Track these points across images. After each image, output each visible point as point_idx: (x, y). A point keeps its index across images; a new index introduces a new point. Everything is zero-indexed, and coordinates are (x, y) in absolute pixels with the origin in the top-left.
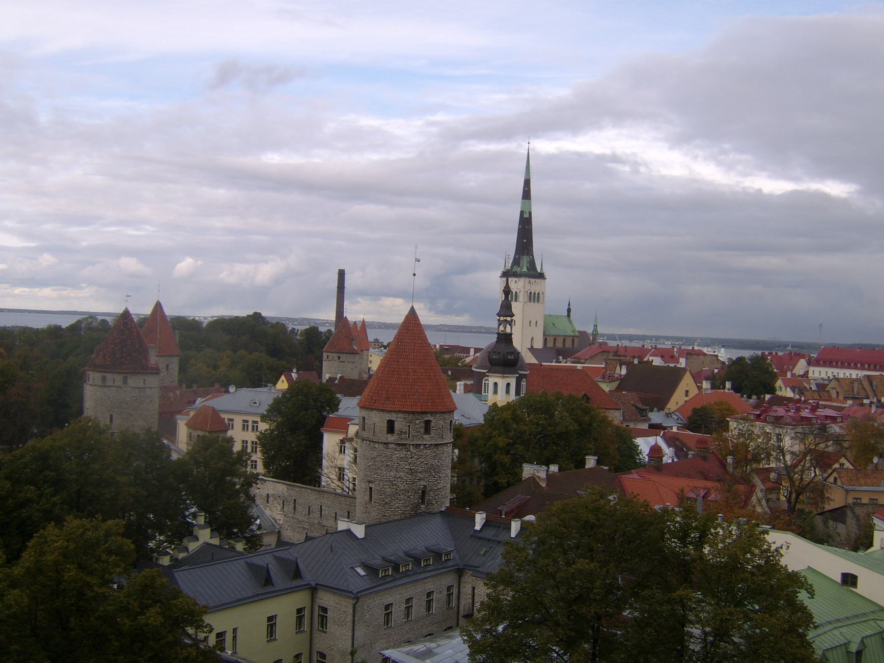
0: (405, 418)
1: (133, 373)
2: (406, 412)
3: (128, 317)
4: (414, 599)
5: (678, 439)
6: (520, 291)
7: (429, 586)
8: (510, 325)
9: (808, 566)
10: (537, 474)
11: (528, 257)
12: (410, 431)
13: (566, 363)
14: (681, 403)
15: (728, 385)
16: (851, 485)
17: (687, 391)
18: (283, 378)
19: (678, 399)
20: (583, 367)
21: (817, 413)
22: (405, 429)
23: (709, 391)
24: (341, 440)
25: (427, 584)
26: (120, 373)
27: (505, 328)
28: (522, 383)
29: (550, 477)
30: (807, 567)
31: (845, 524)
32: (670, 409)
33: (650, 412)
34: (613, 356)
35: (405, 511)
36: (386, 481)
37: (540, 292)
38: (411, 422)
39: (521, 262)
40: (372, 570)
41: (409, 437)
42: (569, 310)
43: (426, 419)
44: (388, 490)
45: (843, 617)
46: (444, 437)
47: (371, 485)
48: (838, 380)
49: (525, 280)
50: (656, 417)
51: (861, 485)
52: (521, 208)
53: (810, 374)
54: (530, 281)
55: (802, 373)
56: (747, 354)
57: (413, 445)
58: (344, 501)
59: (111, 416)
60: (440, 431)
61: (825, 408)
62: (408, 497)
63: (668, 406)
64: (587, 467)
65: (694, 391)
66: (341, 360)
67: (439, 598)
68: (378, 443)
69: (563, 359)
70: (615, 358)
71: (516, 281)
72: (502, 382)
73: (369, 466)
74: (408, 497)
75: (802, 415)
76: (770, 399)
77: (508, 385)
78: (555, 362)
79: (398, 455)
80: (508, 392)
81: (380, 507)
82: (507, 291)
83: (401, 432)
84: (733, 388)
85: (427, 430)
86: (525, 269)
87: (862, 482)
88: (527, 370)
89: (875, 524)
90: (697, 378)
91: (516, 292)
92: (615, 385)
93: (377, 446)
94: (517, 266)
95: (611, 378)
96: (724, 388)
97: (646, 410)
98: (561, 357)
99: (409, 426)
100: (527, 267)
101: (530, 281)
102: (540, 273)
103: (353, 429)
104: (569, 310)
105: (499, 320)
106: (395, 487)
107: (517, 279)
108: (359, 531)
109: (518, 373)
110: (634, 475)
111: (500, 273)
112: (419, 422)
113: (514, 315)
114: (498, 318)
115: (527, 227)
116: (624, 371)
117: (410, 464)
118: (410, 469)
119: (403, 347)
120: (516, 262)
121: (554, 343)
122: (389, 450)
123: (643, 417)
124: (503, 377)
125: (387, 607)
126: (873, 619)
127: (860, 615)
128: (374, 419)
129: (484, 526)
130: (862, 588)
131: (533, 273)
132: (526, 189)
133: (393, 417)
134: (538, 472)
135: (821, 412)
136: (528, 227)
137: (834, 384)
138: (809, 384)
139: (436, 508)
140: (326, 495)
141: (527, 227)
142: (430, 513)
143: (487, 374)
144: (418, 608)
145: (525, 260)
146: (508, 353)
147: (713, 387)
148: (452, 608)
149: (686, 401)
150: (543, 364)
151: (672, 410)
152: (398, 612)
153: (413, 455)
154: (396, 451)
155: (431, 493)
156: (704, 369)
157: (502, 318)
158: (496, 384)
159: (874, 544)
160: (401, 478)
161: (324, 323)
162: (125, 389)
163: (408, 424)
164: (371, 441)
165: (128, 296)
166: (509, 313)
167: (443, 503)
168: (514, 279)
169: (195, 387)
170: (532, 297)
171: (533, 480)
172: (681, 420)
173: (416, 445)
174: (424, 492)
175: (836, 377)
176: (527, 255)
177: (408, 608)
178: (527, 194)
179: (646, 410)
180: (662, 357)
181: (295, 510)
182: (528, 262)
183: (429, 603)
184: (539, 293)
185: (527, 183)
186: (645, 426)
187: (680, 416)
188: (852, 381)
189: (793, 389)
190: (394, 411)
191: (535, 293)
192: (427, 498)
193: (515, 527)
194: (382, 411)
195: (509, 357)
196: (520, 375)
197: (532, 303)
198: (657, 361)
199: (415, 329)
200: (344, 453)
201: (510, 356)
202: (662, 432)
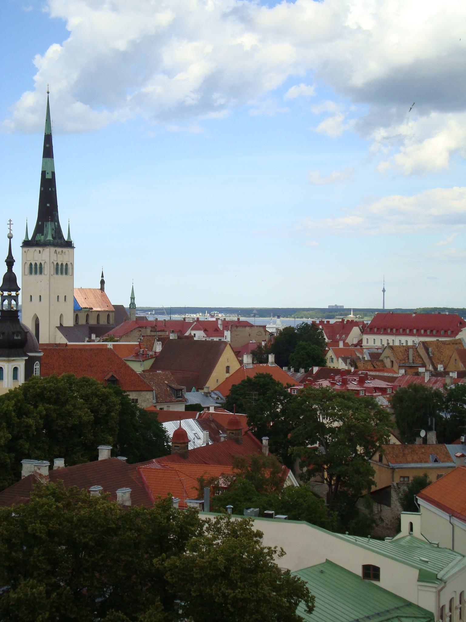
5: (213, 421)
6: (45, 262)
8: (15, 300)
9: (327, 560)
10: (38, 471)
11: (53, 224)
13: (99, 341)
16: (396, 462)
17: (228, 368)
21: (365, 385)
23: (251, 366)
27: (10, 304)
28: (35, 367)
29: (53, 474)
30: (325, 561)
31: (389, 505)
32: (208, 388)
33: (187, 392)
34: (151, 331)
37: (69, 263)
42: (102, 282)
45: (362, 616)
48: (391, 348)
49: (50, 249)
51: (408, 462)
52: (43, 167)
53: (364, 343)
54: (56, 250)
55: (355, 342)
56: (294, 322)
61: (374, 379)
63: (207, 385)
64: (100, 458)
65: (235, 366)
69: (96, 337)
70: (153, 334)
71: (40, 251)
75: (349, 388)
76: (318, 372)
77: (16, 369)
78: (88, 341)
80: (15, 377)
82: (10, 262)
84: (277, 361)
86: (50, 238)
87: (409, 458)
88: (40, 352)
89: (419, 505)
91: (41, 264)
92: (148, 364)
94: (41, 234)
95: (145, 356)
96: (266, 361)
97: (181, 390)
98: (93, 336)
100: (52, 235)
101: (56, 250)
102: (67, 242)
104: (102, 282)
105: (2, 295)
107: (41, 249)
109: (26, 355)
110: (155, 464)
113: (19, 289)
114: (2, 293)
115: (50, 189)
120: (39, 229)
124: (9, 361)
126: (397, 617)
127: (382, 613)
130: (385, 582)
131: (59, 241)
132: (47, 146)
134: (39, 469)
136: (52, 189)
137: (388, 352)
138: (362, 353)
141: (50, 189)
145: (49, 228)
146: (13, 333)
150: (69, 343)
151: (210, 389)
156: (251, 342)
157: (6, 293)
159: (402, 528)
168: (38, 249)
170: (59, 269)
171: (32, 478)
172: (221, 399)
175: (391, 344)
176: (52, 221)
178: (48, 152)
179: (181, 390)
180: (205, 331)
182: (53, 229)
184: (67, 264)
185: (48, 139)
186: (181, 408)
187: (221, 395)
188: (407, 349)
189: (345, 360)
191: (62, 264)
195: (16, 338)
196: (30, 357)
197: (38, 275)
198: (199, 335)
201: (16, 336)
202: (198, 414)
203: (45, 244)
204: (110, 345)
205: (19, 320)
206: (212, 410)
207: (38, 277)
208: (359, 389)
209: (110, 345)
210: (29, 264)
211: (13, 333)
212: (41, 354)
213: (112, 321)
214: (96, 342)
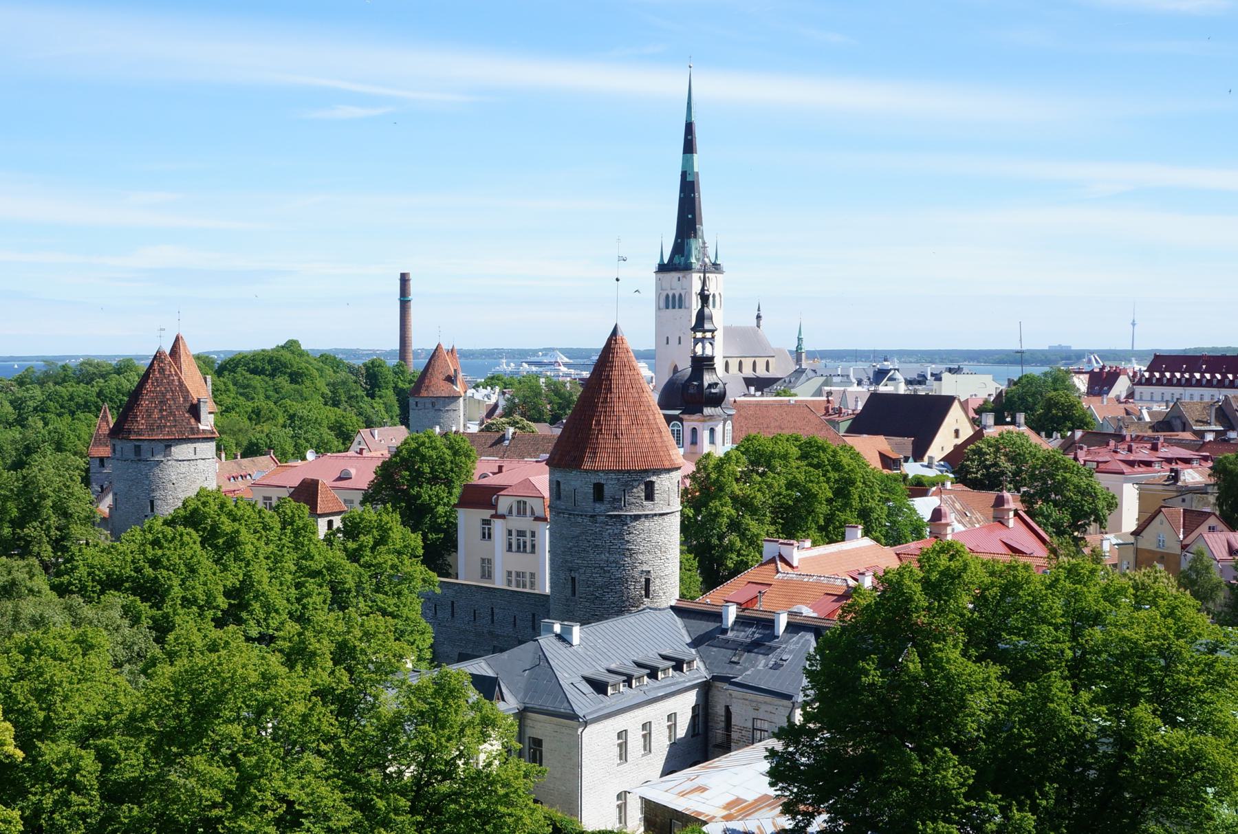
0: (619, 480)
4: (653, 724)
8: (711, 344)
12: (627, 497)
14: (949, 449)
15: (1021, 417)
17: (957, 432)
19: (943, 443)
24: (483, 520)
27: (704, 348)
32: (931, 458)
35: (624, 607)
36: (595, 568)
38: (626, 484)
40: (600, 687)
41: (625, 506)
42: (759, 317)
46: (671, 503)
50: (912, 469)
53: (1137, 396)
56: (1036, 371)
57: (631, 516)
58: (527, 600)
60: (665, 495)
63: (930, 453)
65: (967, 432)
66: (436, 407)
68: (581, 515)
69: (757, 390)
73: (570, 548)
75: (1138, 459)
76: (1083, 436)
79: (611, 531)
81: (587, 604)
83: (614, 499)
91: (680, 295)
92: (844, 426)
93: (579, 520)
98: (752, 389)
99: (624, 490)
103: (504, 504)
104: (759, 317)
106: (608, 575)
107: (680, 275)
111: (654, 267)
117: (628, 542)
118: (628, 549)
120: (681, 248)
121: (740, 370)
122: (597, 525)
123: (896, 469)
124: (704, 421)
128: (573, 483)
129: (735, 622)
132: (689, 137)
133: (601, 478)
135: (1166, 451)
143: (681, 416)
145: (695, 245)
146: (710, 386)
147: (999, 421)
148: (698, 734)
149: (957, 447)
150: (738, 399)
152: (635, 741)
153: (632, 530)
154: (607, 525)
155: (657, 581)
157: (699, 335)
160: (617, 563)
161: (389, 354)
163: (623, 488)
164: (570, 514)
173: (635, 515)
177: (647, 738)
181: (453, 615)
183: (672, 728)
184: (714, 296)
195: (713, 391)
198: (902, 389)
199: (623, 355)
204: (793, 399)
205: (715, 369)
208: (1154, 459)
209: (793, 399)
210: (664, 294)
212: (733, 412)
214: (758, 398)
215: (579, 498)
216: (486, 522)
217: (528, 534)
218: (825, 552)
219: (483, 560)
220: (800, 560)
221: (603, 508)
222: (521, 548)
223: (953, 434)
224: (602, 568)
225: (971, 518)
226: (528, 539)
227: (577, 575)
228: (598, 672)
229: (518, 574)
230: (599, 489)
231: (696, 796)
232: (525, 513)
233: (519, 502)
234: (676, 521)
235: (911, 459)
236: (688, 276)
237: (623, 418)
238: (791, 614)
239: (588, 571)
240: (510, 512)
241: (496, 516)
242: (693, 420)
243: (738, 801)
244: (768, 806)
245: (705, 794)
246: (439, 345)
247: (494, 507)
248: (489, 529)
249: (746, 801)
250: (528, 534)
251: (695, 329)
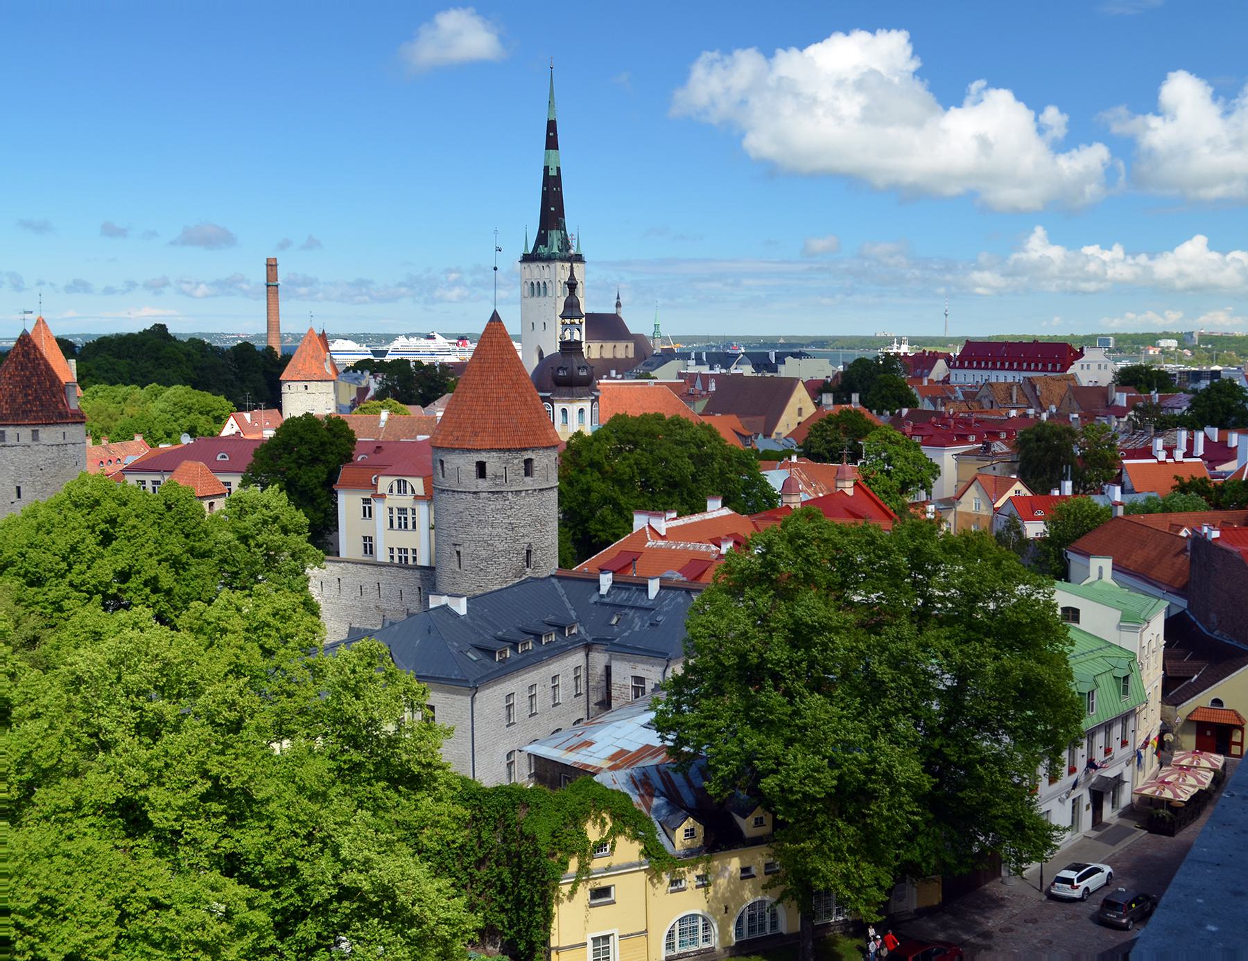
1: (46, 424)
2: (500, 450)
3: (29, 343)
7: (555, 667)
14: (794, 426)
17: (800, 409)
18: (232, 420)
19: (788, 422)
20: (655, 384)
22: (501, 472)
23: (831, 408)
25: (551, 667)
26: (24, 425)
27: (572, 334)
32: (778, 434)
38: (507, 462)
39: (549, 239)
42: (618, 305)
43: (526, 457)
44: (484, 552)
47: (458, 548)
50: (761, 444)
52: (545, 162)
59: (18, 488)
62: (510, 559)
63: (777, 430)
66: (309, 391)
67: (566, 682)
72: (573, 408)
74: (510, 559)
77: (581, 411)
84: (861, 401)
85: (528, 473)
86: (556, 250)
90: (816, 389)
93: (463, 496)
98: (613, 373)
104: (618, 305)
105: (563, 324)
106: (491, 548)
107: (545, 265)
108: (461, 607)
112: (518, 461)
116: (712, 387)
117: (509, 517)
119: (487, 365)
120: (542, 239)
124: (571, 402)
125: (509, 696)
128: (457, 461)
129: (612, 587)
132: (551, 134)
133: (482, 457)
139: (544, 573)
140: (383, 569)
142: (537, 579)
144: (543, 698)
145: (554, 236)
148: (580, 694)
149: (799, 423)
151: (784, 435)
152: (520, 702)
157: (568, 321)
158: (564, 411)
160: (500, 536)
162: (36, 448)
165: (25, 312)
166: (578, 314)
167: (551, 565)
168: (541, 265)
169: (104, 442)
174: (529, 552)
178: (552, 143)
185: (552, 126)
190: (485, 450)
192: (533, 559)
193: (654, 587)
194: (469, 450)
195: (581, 374)
198: (747, 370)
200: (370, 516)
203: (550, 259)
206: (794, 459)
207: (541, 300)
210: (529, 283)
211: (579, 368)
213: (631, 355)
215: (462, 476)
216: (366, 501)
217: (410, 512)
218: (690, 521)
219: (365, 538)
220: (667, 530)
221: (486, 484)
222: (403, 525)
223: (797, 412)
224: (486, 542)
225: (815, 488)
226: (410, 515)
227: (461, 549)
228: (487, 639)
229: (400, 550)
230: (481, 469)
231: (584, 751)
232: (405, 492)
233: (399, 481)
234: (555, 495)
235: (760, 436)
236: (552, 265)
237: (503, 400)
238: (661, 579)
239: (473, 544)
240: (391, 491)
241: (376, 496)
242: (563, 401)
243: (623, 752)
244: (651, 755)
245: (592, 748)
246: (311, 330)
247: (375, 487)
248: (370, 508)
249: (629, 752)
250: (410, 512)
251: (563, 317)
